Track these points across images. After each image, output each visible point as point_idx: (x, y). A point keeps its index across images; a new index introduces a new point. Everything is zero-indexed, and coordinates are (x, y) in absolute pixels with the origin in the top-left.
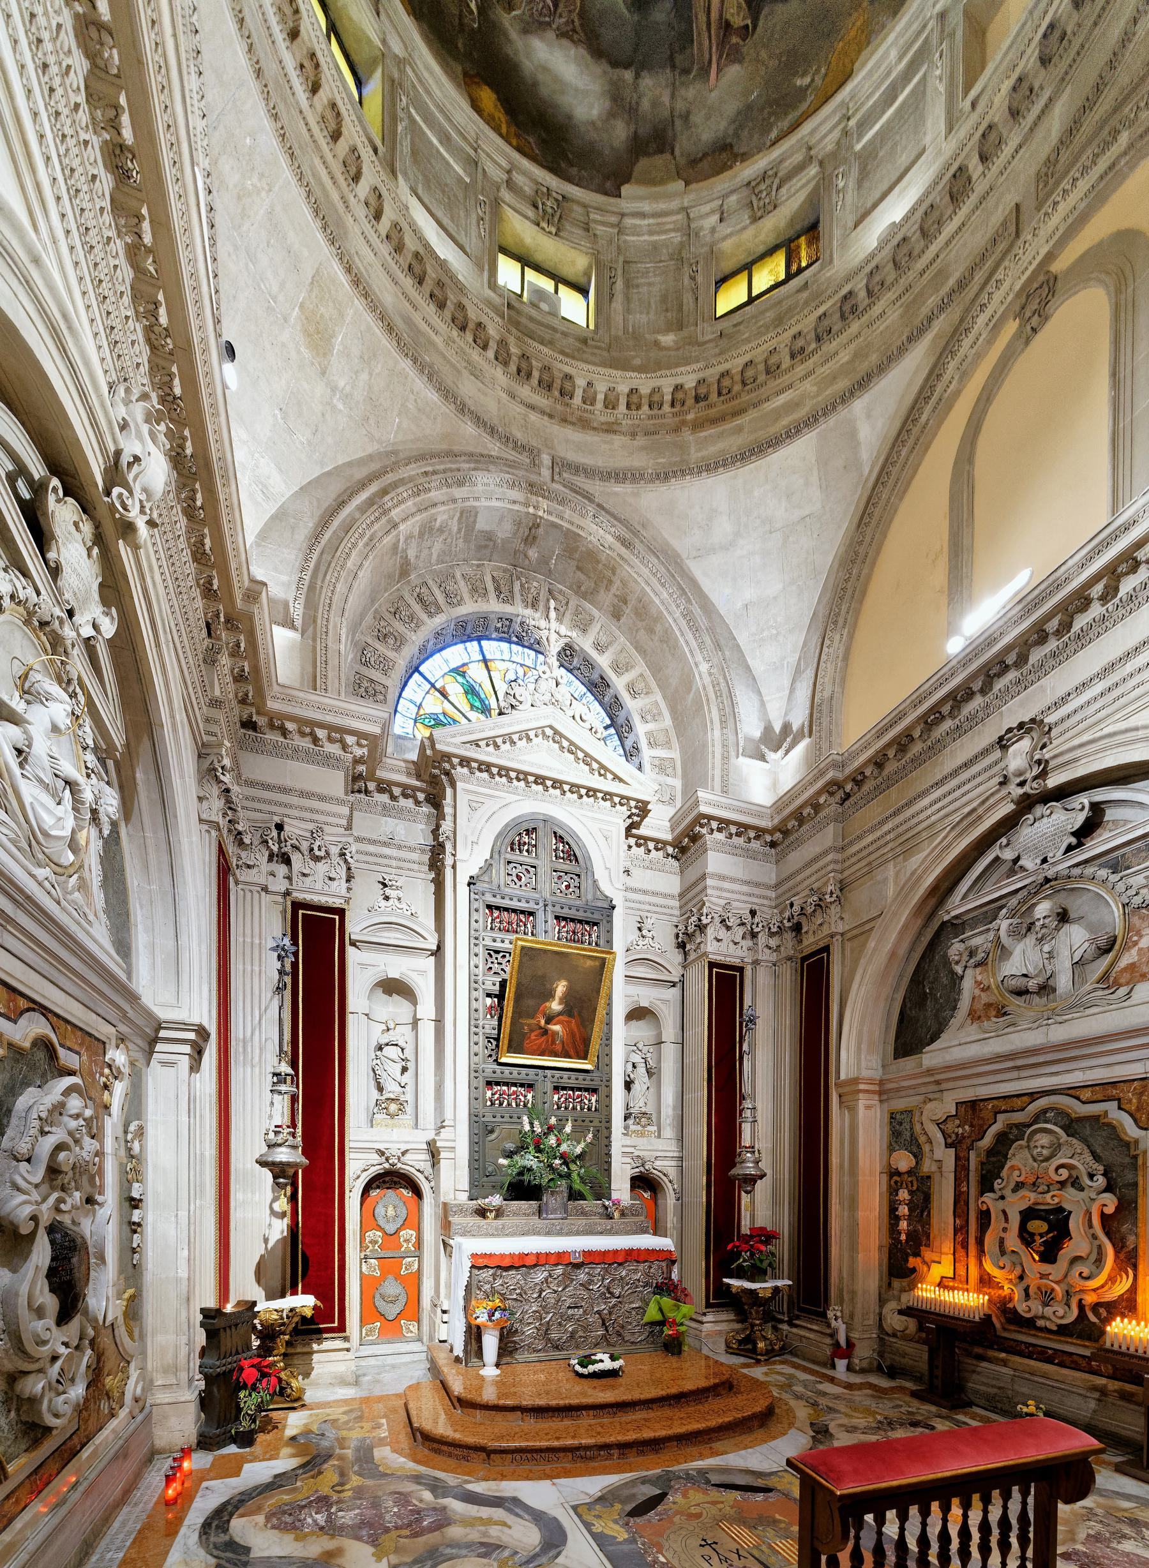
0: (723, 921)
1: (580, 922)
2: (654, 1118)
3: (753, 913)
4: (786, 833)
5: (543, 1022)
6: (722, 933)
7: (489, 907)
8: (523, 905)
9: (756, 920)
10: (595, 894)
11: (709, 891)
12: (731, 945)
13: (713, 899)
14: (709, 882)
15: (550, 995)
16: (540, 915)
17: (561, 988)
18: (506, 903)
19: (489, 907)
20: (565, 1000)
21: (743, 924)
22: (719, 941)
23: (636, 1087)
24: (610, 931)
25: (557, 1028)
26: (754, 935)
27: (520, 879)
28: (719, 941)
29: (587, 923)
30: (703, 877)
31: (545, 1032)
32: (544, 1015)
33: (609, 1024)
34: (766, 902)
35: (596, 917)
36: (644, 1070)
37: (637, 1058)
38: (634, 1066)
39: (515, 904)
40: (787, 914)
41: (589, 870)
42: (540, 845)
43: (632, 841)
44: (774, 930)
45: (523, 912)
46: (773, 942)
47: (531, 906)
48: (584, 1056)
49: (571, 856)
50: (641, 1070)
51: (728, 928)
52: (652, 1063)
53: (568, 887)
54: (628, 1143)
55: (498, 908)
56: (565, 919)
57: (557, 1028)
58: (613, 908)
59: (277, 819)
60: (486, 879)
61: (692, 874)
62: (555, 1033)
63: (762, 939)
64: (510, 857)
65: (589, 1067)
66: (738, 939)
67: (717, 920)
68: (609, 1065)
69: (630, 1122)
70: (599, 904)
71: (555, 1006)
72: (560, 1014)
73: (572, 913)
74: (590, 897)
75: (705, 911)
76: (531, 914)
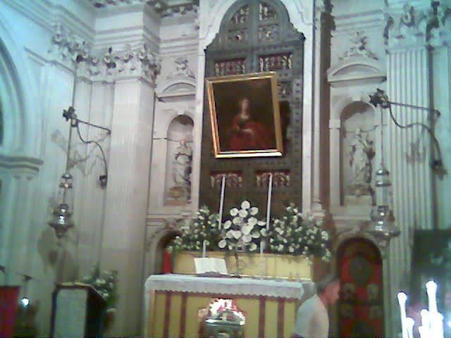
5: (238, 128)
6: (404, 30)
15: (238, 110)
17: (244, 104)
20: (249, 111)
25: (248, 130)
31: (240, 135)
57: (248, 130)
59: (109, 47)
62: (248, 135)
65: (279, 154)
71: (244, 116)
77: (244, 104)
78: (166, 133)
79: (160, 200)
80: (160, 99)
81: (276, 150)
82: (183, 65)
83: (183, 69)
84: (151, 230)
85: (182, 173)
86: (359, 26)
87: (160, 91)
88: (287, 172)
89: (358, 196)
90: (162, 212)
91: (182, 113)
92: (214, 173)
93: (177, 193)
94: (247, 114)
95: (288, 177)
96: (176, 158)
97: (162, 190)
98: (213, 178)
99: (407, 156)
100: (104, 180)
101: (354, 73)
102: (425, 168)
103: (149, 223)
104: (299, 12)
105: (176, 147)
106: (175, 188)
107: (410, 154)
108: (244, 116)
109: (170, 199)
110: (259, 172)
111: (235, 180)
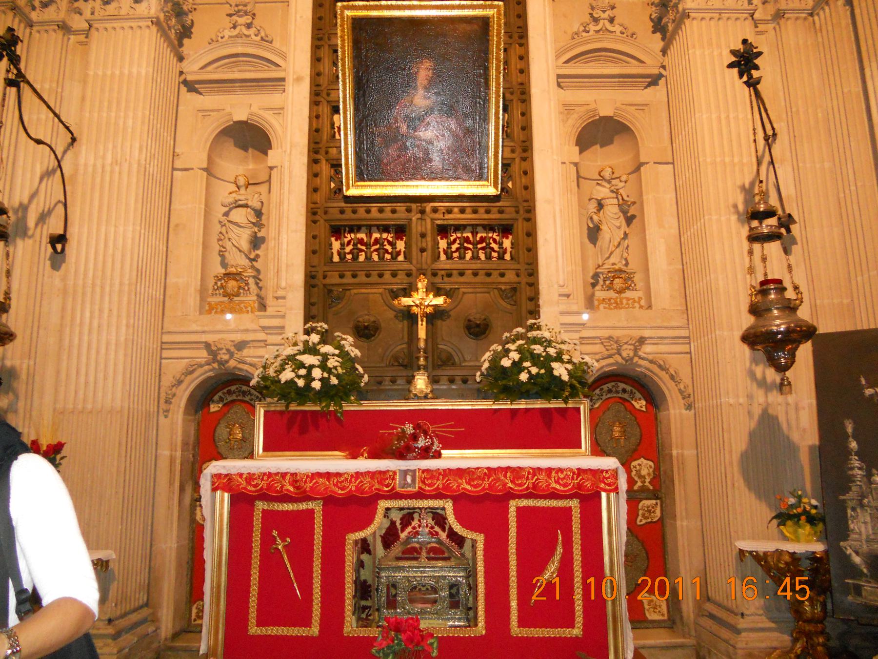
50: (612, 209)
78: (204, 156)
79: (193, 300)
80: (191, 86)
82: (247, 19)
83: (249, 26)
84: (174, 367)
85: (245, 245)
87: (192, 68)
88: (506, 230)
89: (620, 292)
90: (194, 327)
91: (243, 117)
92: (337, 232)
93: (232, 284)
95: (507, 243)
96: (226, 214)
97: (195, 283)
98: (336, 245)
99: (735, 206)
100: (59, 247)
103: (165, 354)
105: (224, 193)
106: (228, 275)
109: (213, 300)
110: (443, 231)
111: (388, 248)
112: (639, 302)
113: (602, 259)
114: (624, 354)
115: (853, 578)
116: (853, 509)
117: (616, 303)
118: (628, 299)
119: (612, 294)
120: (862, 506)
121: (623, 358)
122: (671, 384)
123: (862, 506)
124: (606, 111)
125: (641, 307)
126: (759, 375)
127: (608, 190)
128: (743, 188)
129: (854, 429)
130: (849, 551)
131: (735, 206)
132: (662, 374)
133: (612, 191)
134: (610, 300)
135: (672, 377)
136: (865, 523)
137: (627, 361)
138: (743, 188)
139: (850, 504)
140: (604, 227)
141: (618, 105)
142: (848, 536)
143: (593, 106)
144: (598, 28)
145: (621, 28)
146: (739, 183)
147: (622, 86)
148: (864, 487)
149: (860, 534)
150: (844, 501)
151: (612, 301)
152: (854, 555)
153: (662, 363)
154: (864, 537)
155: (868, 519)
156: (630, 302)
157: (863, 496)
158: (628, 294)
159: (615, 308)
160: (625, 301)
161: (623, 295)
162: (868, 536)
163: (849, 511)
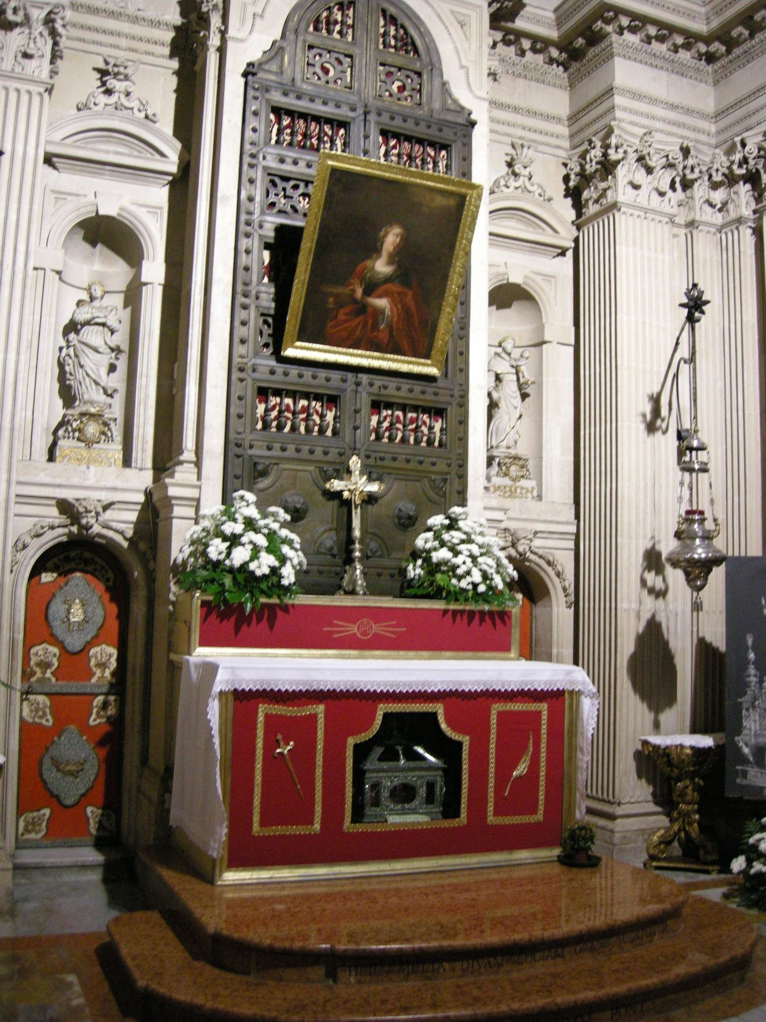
0: (641, 159)
1: (420, 141)
2: (531, 464)
3: (686, 151)
4: (731, 44)
5: (359, 292)
6: (640, 176)
7: (277, 111)
8: (328, 110)
9: (690, 162)
10: (444, 102)
11: (618, 114)
12: (655, 195)
13: (624, 125)
14: (618, 100)
15: (375, 249)
16: (357, 130)
17: (392, 238)
18: (303, 105)
19: (277, 111)
20: (400, 256)
21: (671, 166)
22: (636, 187)
23: (503, 416)
24: (467, 159)
25: (382, 303)
26: (687, 185)
27: (326, 71)
28: (636, 187)
29: (432, 144)
30: (609, 92)
31: (362, 309)
32: (362, 280)
33: (465, 303)
34: (704, 138)
35: (447, 135)
36: (514, 387)
37: (503, 367)
38: (498, 378)
39: (318, 108)
40: (737, 157)
41: (435, 66)
42: (358, 26)
43: (499, 36)
44: (718, 178)
45: (329, 121)
46: (718, 196)
47: (343, 113)
48: (425, 354)
49: (407, 44)
50: (510, 387)
51: (649, 170)
52: (527, 374)
53: (402, 89)
54: (494, 503)
55: (290, 113)
56: (396, 136)
57: (382, 303)
58: (473, 124)
60: (274, 67)
61: (591, 88)
62: (378, 312)
63: (700, 190)
64: (311, 39)
65: (434, 371)
66: (665, 186)
67: (633, 157)
68: (464, 370)
69: (495, 468)
70: (450, 117)
71: (382, 267)
72: (388, 280)
73: (409, 127)
74: (437, 106)
75: (613, 141)
76: (343, 124)
77: (392, 238)
81: (429, 362)
86: (519, 132)
89: (514, 480)
94: (390, 262)
99: (644, 416)
101: (513, 223)
102: (670, 442)
104: (462, 67)
107: (649, 417)
108: (382, 267)
112: (532, 492)
113: (496, 439)
114: (521, 549)
115: (742, 765)
116: (747, 710)
117: (510, 490)
118: (522, 488)
119: (506, 481)
120: (753, 707)
121: (517, 552)
122: (556, 580)
123: (753, 707)
124: (516, 278)
125: (533, 498)
126: (650, 583)
127: (508, 365)
128: (651, 398)
129: (753, 642)
130: (741, 744)
131: (644, 416)
132: (549, 570)
133: (513, 366)
134: (505, 487)
135: (558, 575)
136: (755, 721)
137: (521, 555)
138: (651, 398)
139: (745, 705)
140: (502, 404)
141: (527, 272)
142: (741, 732)
143: (502, 269)
144: (517, 184)
145: (540, 191)
146: (649, 392)
147: (533, 251)
148: (757, 692)
149: (750, 729)
150: (741, 704)
151: (507, 489)
152: (744, 747)
153: (551, 559)
154: (753, 732)
155: (757, 718)
156: (524, 491)
157: (755, 699)
158: (523, 483)
159: (509, 496)
160: (519, 490)
161: (518, 484)
162: (755, 732)
163: (744, 711)
